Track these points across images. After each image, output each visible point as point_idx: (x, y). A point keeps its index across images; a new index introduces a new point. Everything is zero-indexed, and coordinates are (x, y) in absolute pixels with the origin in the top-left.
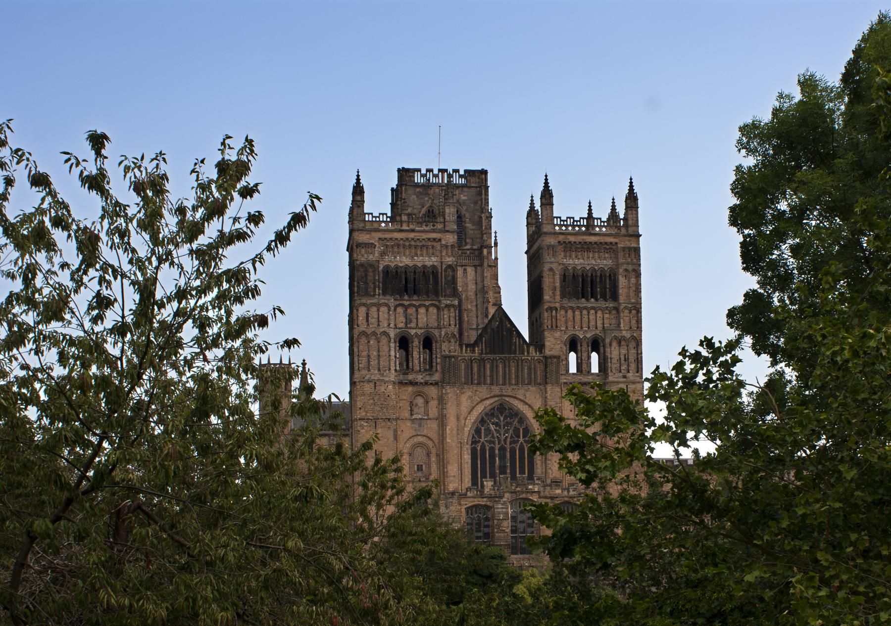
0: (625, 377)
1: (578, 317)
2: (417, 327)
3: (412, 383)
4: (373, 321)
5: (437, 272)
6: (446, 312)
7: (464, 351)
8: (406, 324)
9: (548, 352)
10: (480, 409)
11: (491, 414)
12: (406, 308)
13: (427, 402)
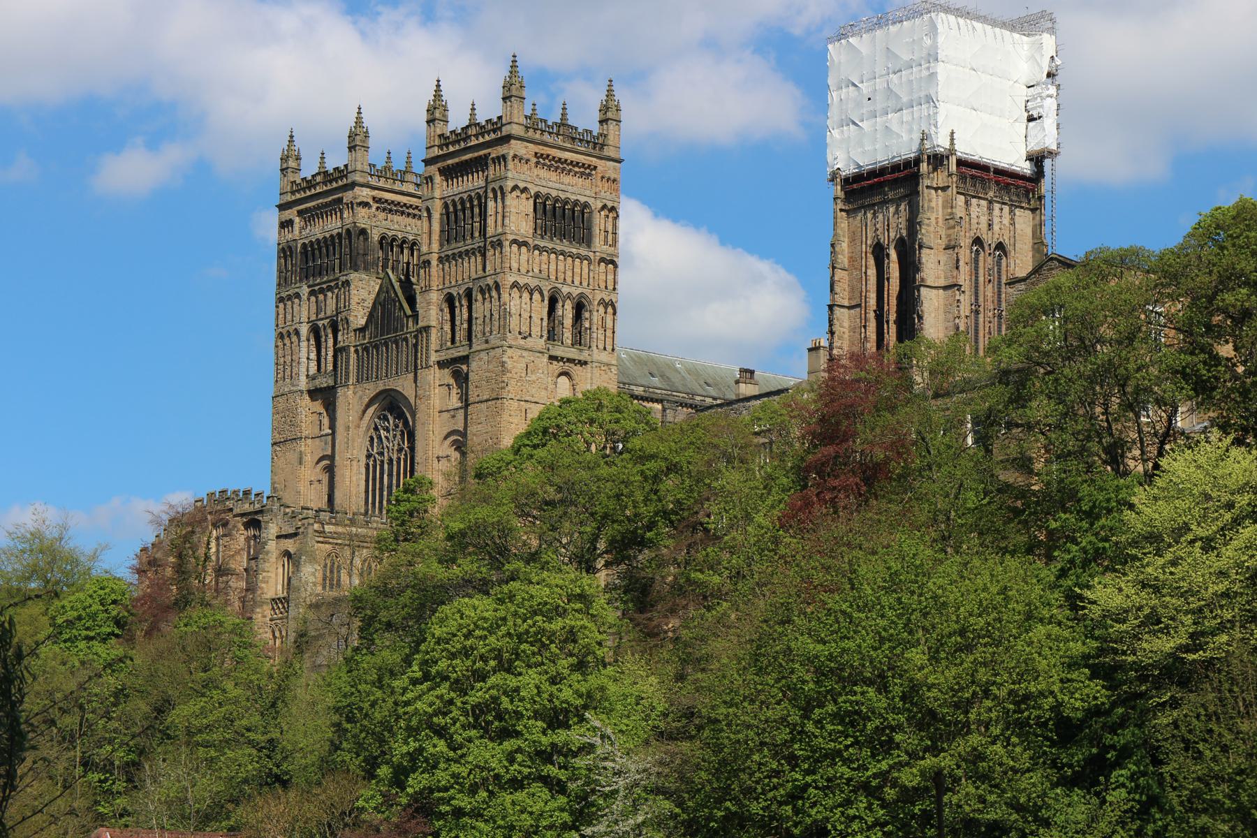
0: (487, 342)
4: (289, 317)
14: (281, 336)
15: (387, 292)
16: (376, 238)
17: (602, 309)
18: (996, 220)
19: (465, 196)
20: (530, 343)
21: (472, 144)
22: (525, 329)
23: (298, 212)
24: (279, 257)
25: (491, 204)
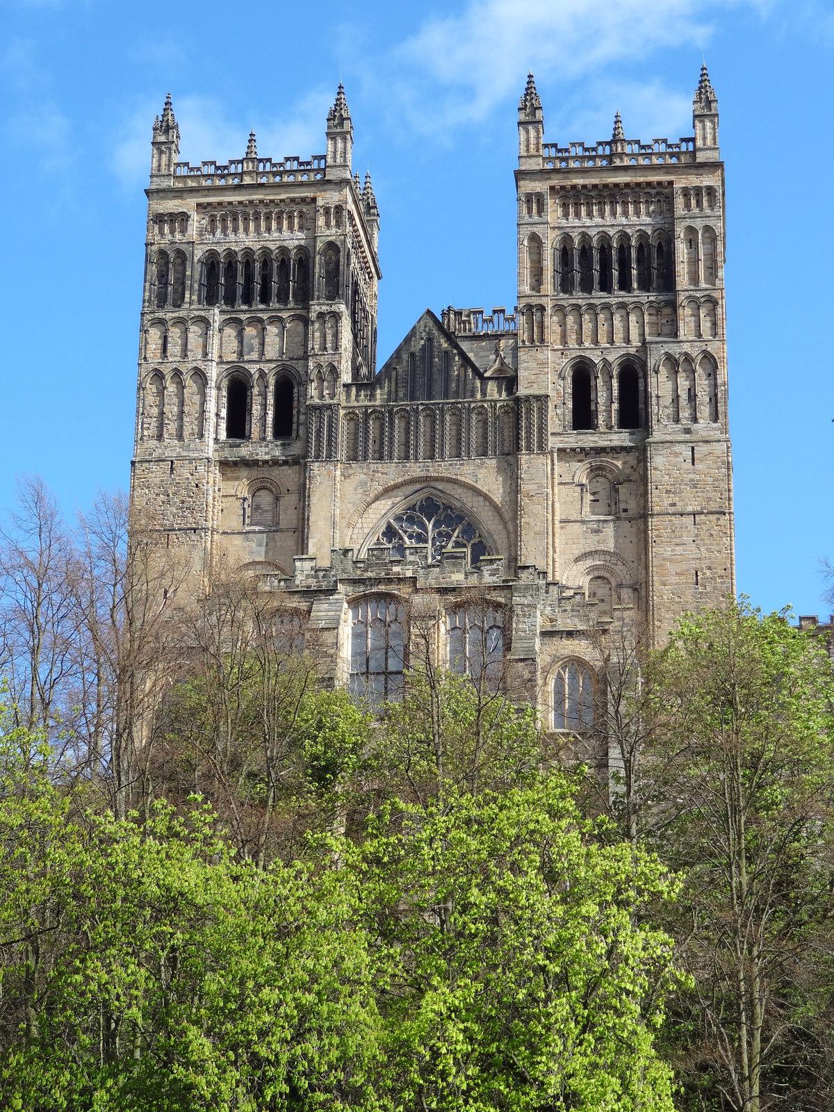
0: (688, 431)
1: (587, 326)
4: (174, 349)
5: (308, 257)
6: (317, 326)
7: (353, 397)
8: (241, 354)
9: (522, 391)
13: (277, 499)
14: (158, 375)
19: (612, 232)
21: (625, 164)
23: (198, 205)
24: (148, 260)
25: (682, 250)
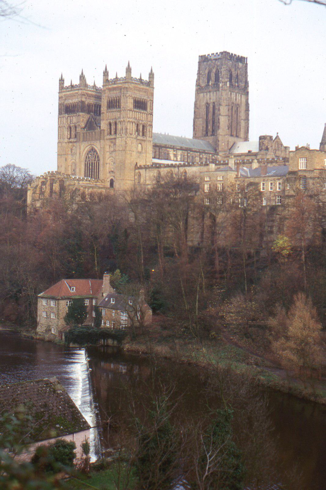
0: (121, 135)
2: (73, 123)
3: (71, 142)
4: (62, 122)
10: (86, 149)
11: (90, 152)
12: (70, 117)
15: (91, 119)
16: (87, 104)
17: (149, 127)
18: (237, 98)
20: (132, 136)
22: (131, 132)
